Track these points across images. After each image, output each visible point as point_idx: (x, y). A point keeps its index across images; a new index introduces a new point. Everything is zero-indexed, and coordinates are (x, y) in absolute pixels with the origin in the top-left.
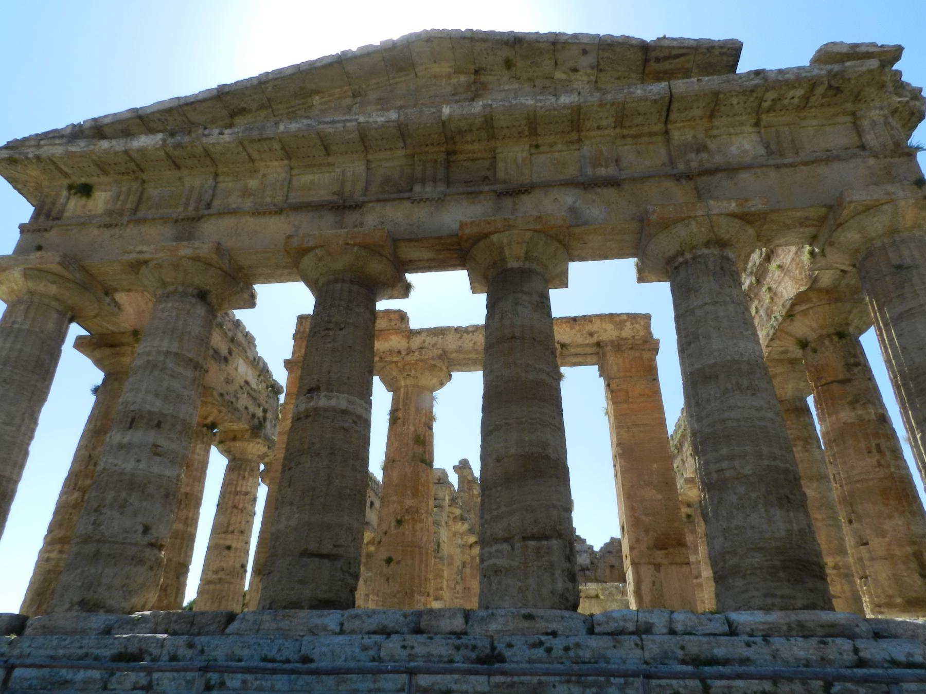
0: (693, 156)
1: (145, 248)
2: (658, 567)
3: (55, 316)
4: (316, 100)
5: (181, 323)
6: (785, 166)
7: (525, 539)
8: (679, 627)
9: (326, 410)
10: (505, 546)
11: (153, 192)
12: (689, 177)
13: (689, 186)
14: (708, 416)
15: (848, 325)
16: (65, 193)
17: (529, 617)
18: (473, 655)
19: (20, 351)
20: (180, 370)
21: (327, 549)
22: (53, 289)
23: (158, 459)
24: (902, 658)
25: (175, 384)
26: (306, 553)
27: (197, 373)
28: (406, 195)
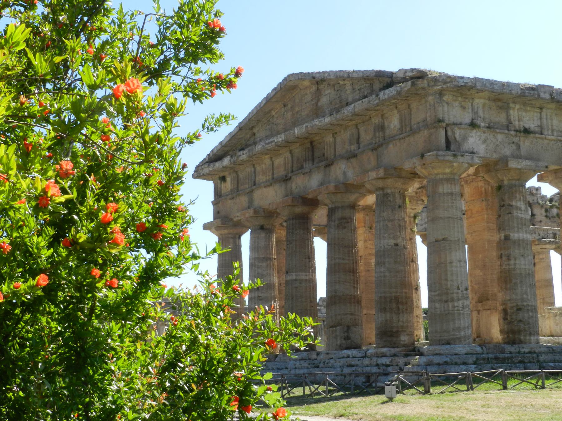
1: (238, 214)
2: (479, 312)
3: (231, 240)
4: (273, 113)
5: (257, 243)
7: (331, 327)
11: (241, 175)
15: (502, 181)
16: (219, 182)
17: (327, 354)
18: (313, 366)
19: (225, 260)
20: (260, 264)
22: (226, 231)
23: (261, 301)
24: (384, 363)
25: (260, 271)
27: (268, 262)
28: (300, 171)
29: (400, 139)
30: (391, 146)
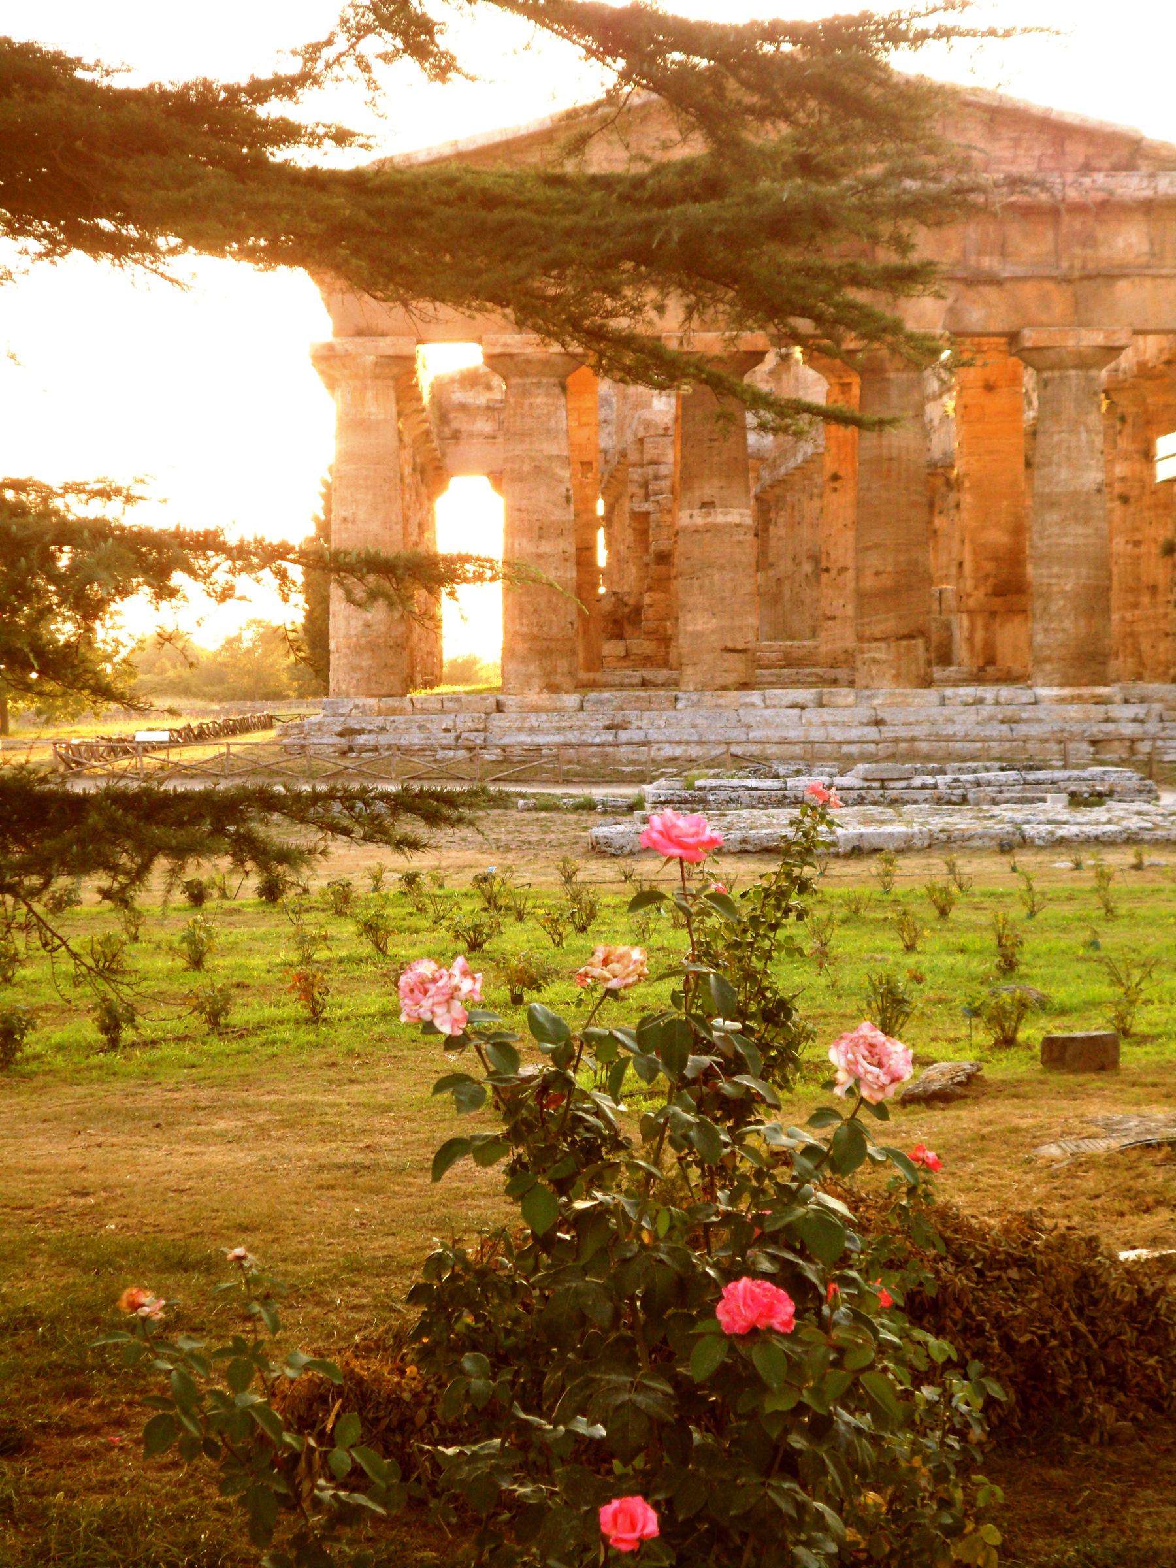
0: (1077, 251)
6: (1161, 277)
7: (899, 639)
8: (1002, 700)
9: (725, 526)
10: (883, 645)
12: (1069, 281)
13: (1069, 290)
14: (1049, 537)
21: (740, 646)
26: (728, 650)
29: (1154, 277)
30: (1122, 285)
